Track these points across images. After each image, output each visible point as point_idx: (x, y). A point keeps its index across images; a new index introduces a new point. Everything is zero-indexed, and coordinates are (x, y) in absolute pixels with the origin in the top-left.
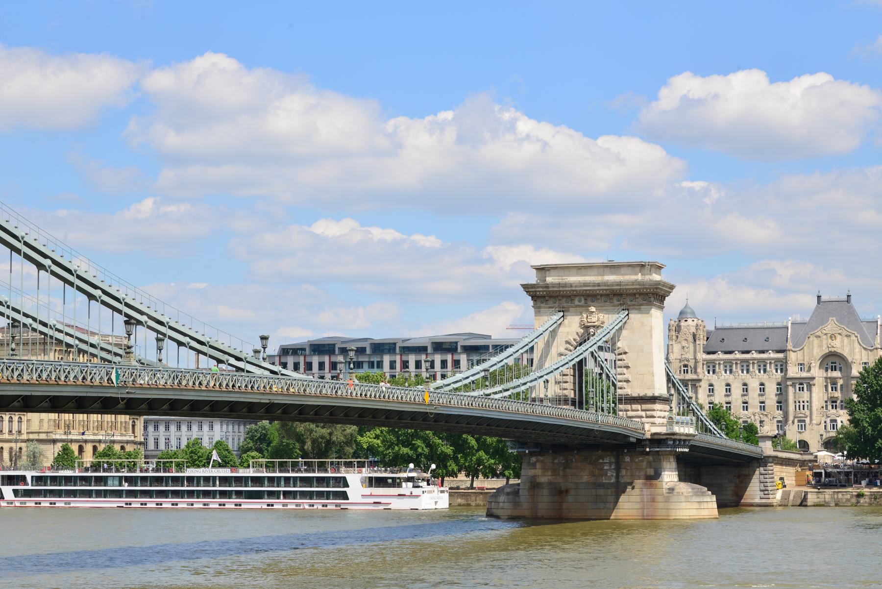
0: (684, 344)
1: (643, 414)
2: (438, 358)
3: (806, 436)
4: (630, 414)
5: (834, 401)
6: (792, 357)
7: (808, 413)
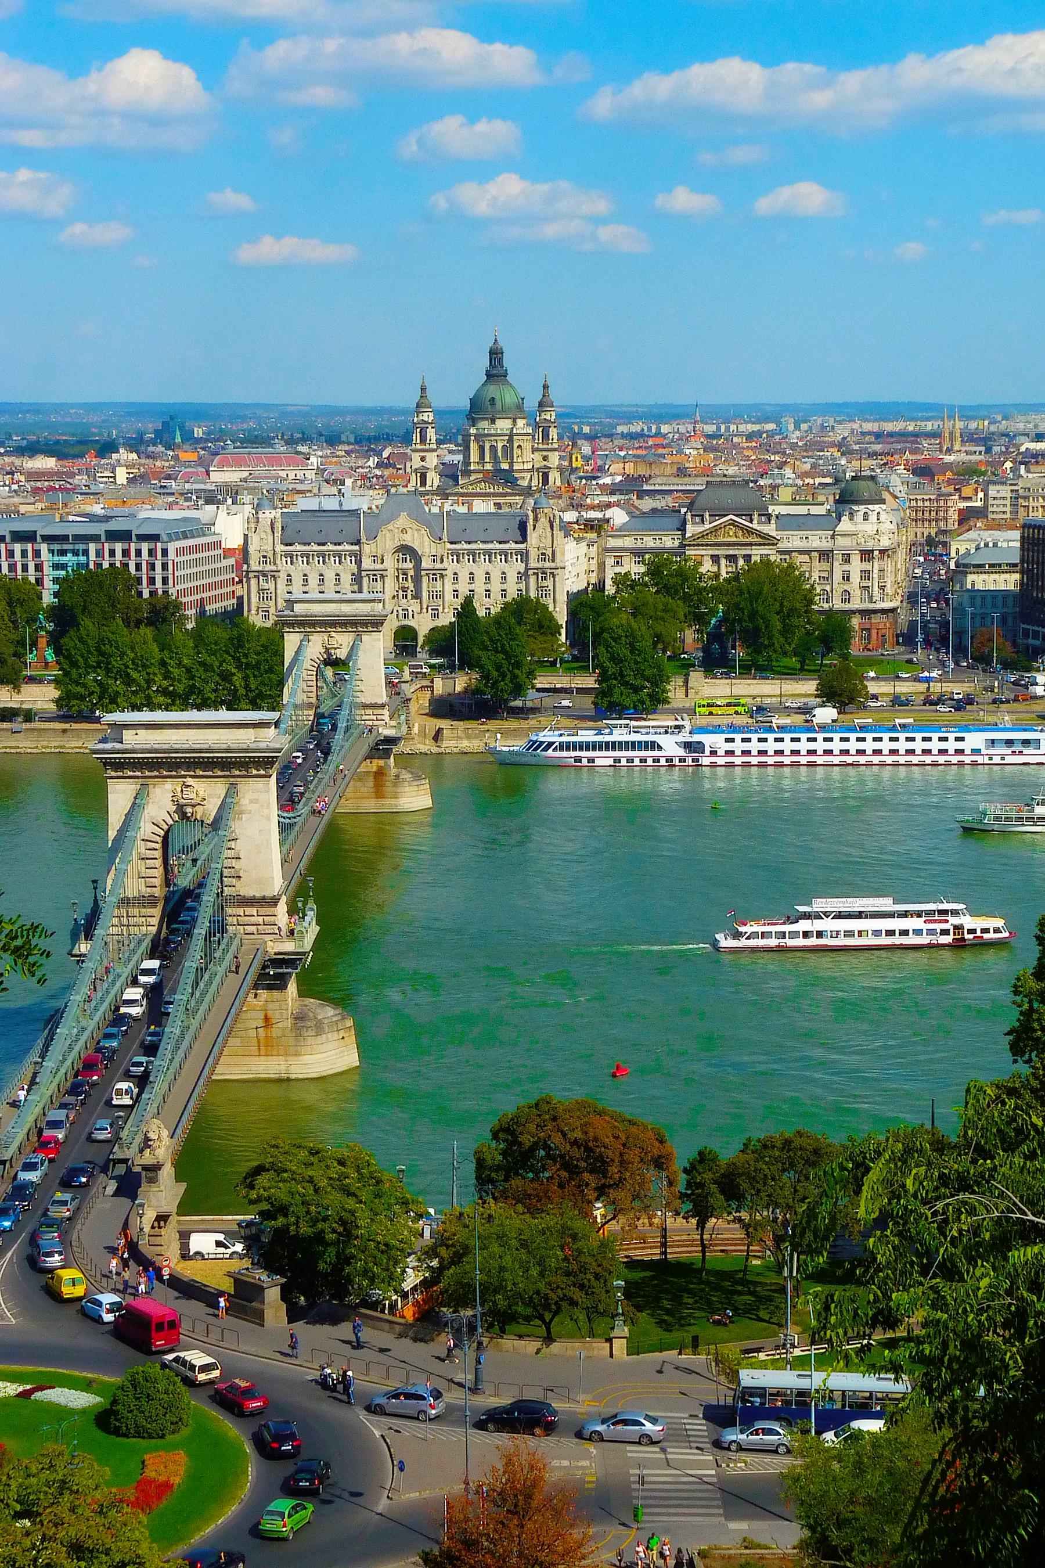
0: (263, 535)
1: (374, 718)
2: (17, 548)
4: (364, 717)
5: (404, 589)
6: (367, 549)
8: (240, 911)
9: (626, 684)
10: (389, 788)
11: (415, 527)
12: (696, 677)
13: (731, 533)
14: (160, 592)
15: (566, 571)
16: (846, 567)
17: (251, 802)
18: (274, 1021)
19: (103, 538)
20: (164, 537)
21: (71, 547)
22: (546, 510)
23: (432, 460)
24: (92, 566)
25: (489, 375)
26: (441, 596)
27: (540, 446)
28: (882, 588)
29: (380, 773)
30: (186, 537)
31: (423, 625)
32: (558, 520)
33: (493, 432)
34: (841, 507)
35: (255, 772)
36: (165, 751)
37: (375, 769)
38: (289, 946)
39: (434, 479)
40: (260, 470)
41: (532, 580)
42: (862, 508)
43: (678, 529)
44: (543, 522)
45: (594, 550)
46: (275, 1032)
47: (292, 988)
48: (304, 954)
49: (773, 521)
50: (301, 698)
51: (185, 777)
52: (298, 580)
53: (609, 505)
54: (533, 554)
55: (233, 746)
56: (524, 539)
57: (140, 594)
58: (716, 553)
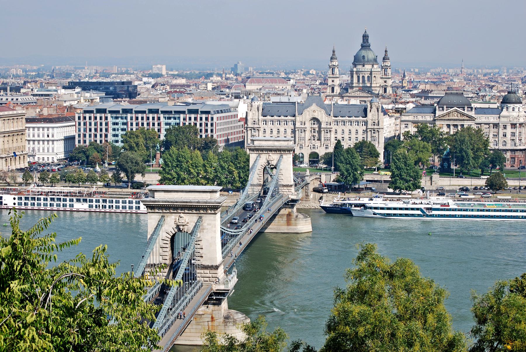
2: (151, 116)
3: (303, 151)
4: (283, 191)
5: (314, 136)
6: (298, 118)
7: (304, 142)
8: (202, 271)
9: (402, 179)
10: (293, 221)
11: (319, 110)
12: (436, 177)
13: (455, 115)
14: (210, 136)
15: (385, 131)
16: (505, 131)
17: (208, 224)
18: (215, 319)
19: (186, 112)
20: (212, 112)
21: (173, 116)
22: (376, 104)
23: (337, 82)
24: (181, 125)
25: (362, 46)
26: (329, 140)
27: (383, 77)
28: (520, 140)
29: (289, 215)
30: (222, 112)
31: (321, 152)
32: (380, 108)
33: (363, 70)
34: (503, 105)
35: (209, 212)
36: (172, 202)
37: (287, 213)
38: (222, 287)
39: (337, 90)
40: (267, 85)
41: (369, 133)
42: (511, 106)
43: (432, 113)
44: (374, 109)
45: (398, 121)
46: (216, 323)
47: (224, 304)
48: (229, 290)
49: (473, 110)
50: (256, 182)
51: (180, 213)
53: (408, 103)
54: (370, 123)
55: (200, 201)
57: (201, 136)
58: (449, 123)
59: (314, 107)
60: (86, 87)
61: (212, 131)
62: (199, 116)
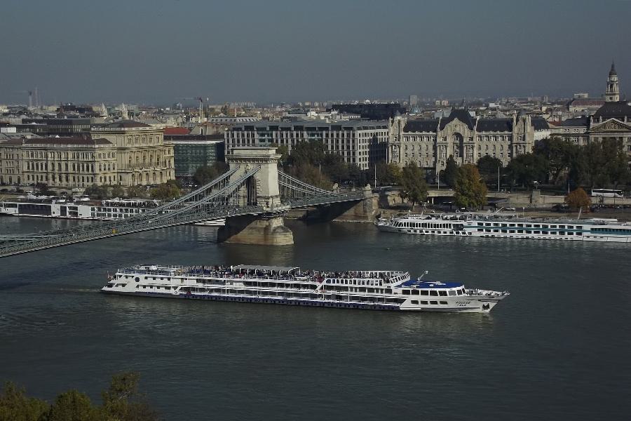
19: (330, 129)
20: (355, 128)
52: (410, 148)
56: (511, 129)
59: (456, 121)
60: (342, 109)
61: (353, 147)
62: (341, 132)
